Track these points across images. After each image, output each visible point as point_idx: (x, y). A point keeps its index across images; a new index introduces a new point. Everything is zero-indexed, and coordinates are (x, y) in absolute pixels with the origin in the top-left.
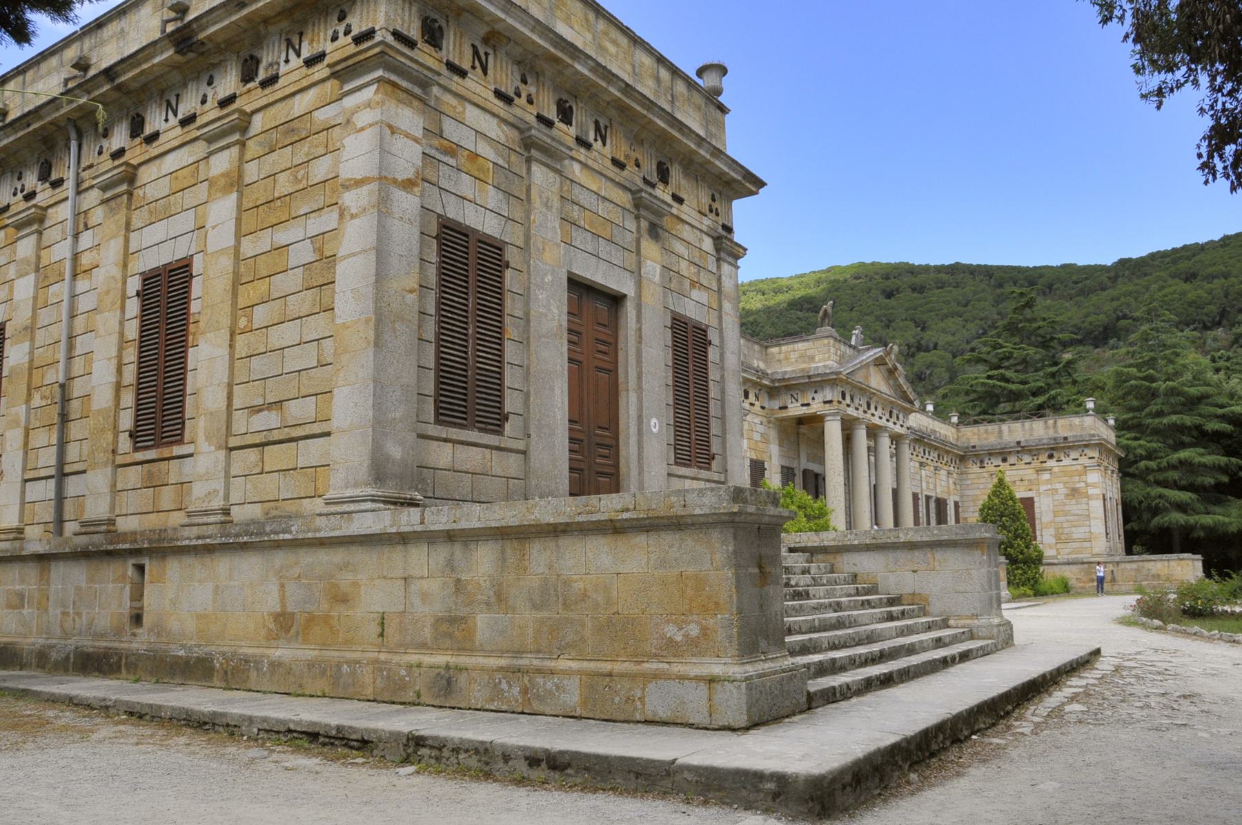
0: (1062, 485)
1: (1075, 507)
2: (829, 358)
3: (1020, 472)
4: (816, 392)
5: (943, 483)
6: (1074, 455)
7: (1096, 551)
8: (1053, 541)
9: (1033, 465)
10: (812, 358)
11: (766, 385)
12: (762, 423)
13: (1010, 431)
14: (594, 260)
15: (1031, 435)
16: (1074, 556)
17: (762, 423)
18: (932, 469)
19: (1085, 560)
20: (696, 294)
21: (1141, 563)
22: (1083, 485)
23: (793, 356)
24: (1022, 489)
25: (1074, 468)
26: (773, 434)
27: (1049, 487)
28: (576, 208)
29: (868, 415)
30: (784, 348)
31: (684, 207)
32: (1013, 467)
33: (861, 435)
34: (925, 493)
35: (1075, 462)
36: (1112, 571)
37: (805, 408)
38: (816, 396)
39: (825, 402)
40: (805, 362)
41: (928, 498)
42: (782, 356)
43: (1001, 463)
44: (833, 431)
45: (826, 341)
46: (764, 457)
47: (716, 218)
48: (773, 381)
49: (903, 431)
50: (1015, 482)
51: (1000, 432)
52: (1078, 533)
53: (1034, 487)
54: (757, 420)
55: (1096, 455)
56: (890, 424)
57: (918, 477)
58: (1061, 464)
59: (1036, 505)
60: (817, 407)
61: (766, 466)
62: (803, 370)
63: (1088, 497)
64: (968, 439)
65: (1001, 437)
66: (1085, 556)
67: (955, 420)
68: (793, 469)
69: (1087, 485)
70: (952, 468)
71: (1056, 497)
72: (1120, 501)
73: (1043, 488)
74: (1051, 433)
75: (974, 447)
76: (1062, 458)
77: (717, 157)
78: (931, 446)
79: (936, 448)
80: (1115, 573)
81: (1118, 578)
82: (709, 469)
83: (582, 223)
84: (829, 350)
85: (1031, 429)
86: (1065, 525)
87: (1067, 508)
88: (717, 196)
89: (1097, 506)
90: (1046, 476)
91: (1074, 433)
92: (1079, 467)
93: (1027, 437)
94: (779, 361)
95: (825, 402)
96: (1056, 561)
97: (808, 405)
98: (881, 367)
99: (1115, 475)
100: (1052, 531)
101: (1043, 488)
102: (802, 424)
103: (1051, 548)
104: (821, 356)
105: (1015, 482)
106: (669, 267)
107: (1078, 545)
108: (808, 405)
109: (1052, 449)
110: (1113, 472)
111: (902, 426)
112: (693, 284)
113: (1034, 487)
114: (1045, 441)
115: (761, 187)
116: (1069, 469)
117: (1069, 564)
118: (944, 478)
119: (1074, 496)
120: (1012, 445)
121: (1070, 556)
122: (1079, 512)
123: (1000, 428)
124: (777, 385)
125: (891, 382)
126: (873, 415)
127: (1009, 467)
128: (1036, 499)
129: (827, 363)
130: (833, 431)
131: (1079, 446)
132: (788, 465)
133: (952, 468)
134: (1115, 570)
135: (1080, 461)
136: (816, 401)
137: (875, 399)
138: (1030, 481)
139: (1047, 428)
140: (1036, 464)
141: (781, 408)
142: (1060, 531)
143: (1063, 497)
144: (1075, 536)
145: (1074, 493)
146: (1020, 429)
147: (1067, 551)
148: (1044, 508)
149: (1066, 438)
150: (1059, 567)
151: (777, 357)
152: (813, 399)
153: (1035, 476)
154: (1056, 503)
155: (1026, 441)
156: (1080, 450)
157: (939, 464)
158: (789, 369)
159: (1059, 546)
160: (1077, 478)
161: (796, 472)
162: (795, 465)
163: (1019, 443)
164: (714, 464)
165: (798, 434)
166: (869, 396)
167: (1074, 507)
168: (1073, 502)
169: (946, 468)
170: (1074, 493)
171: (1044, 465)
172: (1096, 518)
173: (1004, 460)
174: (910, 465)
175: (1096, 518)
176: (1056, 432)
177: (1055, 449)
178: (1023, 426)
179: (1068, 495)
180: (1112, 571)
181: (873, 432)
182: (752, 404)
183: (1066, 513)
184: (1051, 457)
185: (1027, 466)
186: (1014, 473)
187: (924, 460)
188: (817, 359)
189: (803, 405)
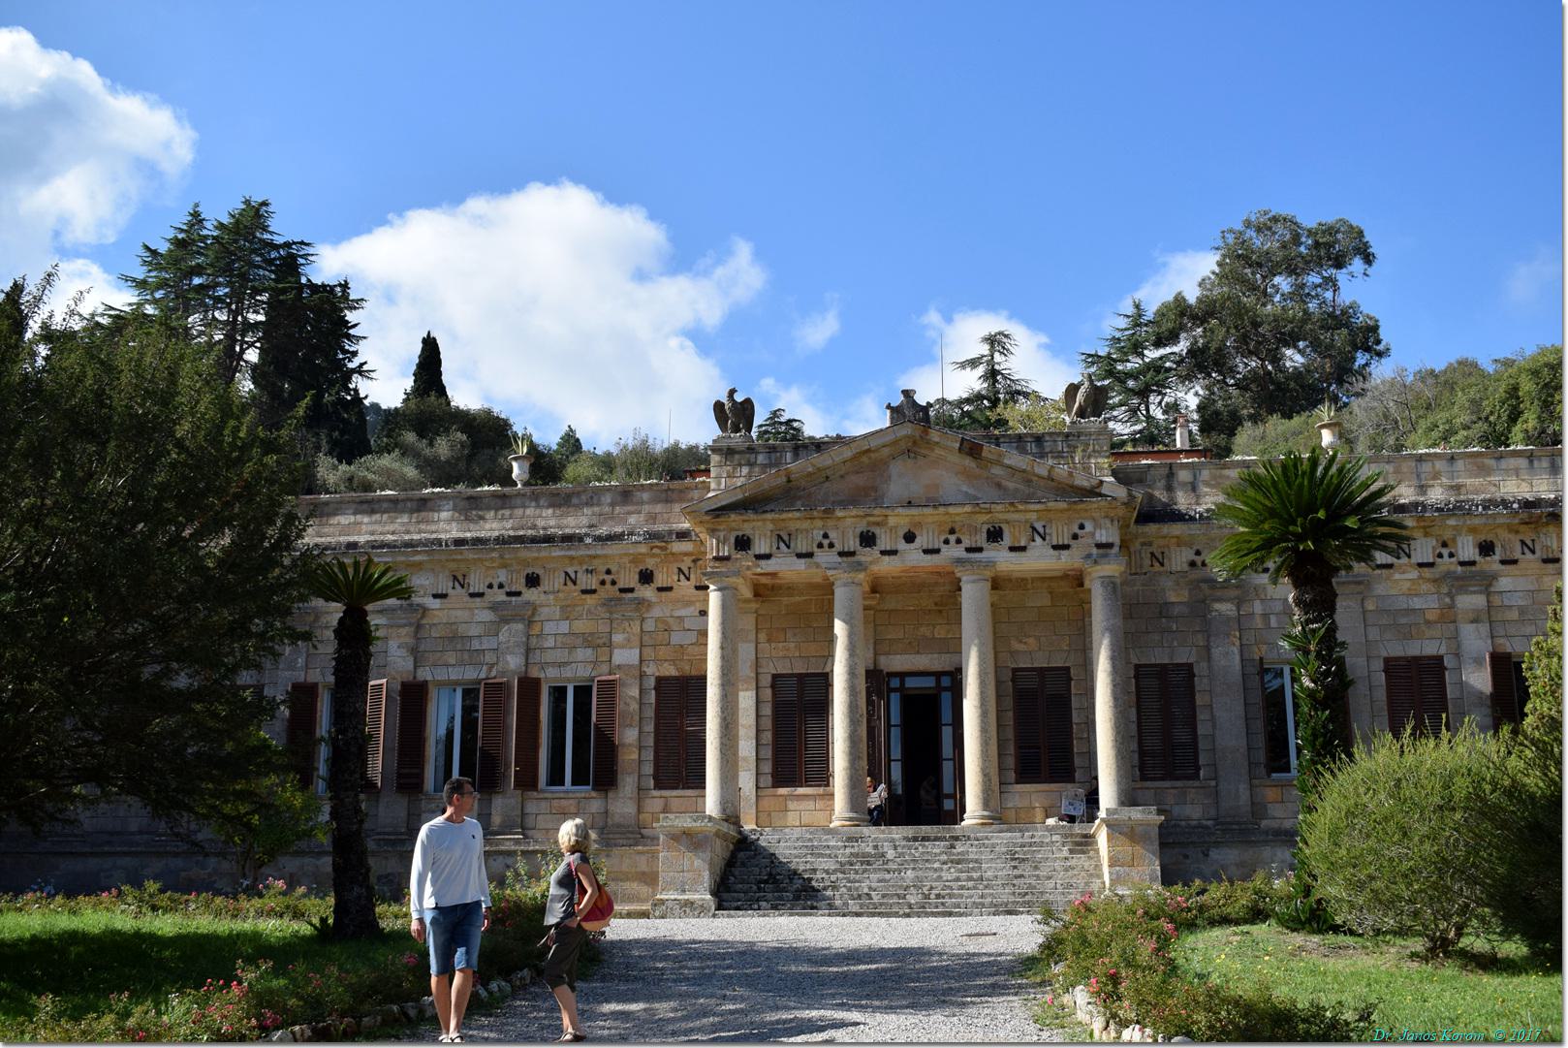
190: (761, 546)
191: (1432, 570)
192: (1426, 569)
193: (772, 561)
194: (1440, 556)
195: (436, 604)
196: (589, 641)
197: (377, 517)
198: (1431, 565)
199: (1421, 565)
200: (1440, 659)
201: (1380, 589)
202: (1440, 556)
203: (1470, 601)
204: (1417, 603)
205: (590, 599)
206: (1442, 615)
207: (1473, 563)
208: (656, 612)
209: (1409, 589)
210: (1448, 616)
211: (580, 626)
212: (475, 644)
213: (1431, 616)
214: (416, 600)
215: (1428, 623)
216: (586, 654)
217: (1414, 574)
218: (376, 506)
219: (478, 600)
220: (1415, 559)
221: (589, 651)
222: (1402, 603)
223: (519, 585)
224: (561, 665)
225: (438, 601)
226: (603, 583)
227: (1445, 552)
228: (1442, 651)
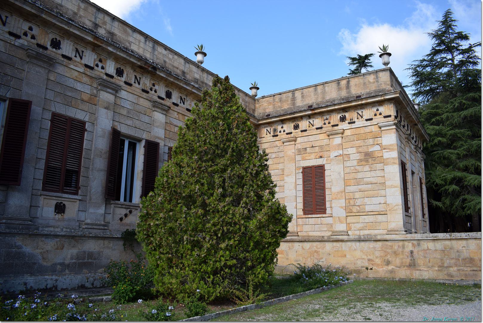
0: (354, 150)
1: (368, 174)
3: (311, 138)
6: (367, 113)
7: (392, 226)
8: (343, 213)
9: (324, 130)
13: (303, 97)
15: (323, 98)
16: (367, 232)
19: (379, 237)
21: (447, 242)
22: (377, 148)
24: (313, 156)
25: (367, 130)
27: (341, 152)
32: (305, 134)
35: (369, 123)
36: (412, 252)
43: (293, 131)
50: (306, 149)
52: (372, 204)
53: (325, 154)
58: (353, 126)
59: (327, 173)
63: (384, 162)
64: (265, 109)
65: (294, 104)
66: (379, 232)
69: (383, 148)
71: (348, 164)
73: (333, 154)
74: (344, 94)
80: (415, 253)
81: (420, 262)
86: (357, 195)
87: (360, 175)
89: (395, 171)
90: (337, 140)
92: (375, 129)
96: (345, 238)
100: (342, 202)
101: (333, 154)
103: (341, 222)
105: (306, 149)
107: (371, 219)
113: (325, 154)
116: (362, 131)
117: (359, 240)
119: (367, 161)
121: (363, 233)
122: (373, 180)
127: (300, 134)
128: (326, 167)
134: (415, 251)
135: (374, 122)
138: (321, 147)
140: (327, 128)
142: (352, 202)
143: (355, 163)
144: (368, 208)
146: (312, 94)
147: (359, 226)
150: (349, 244)
153: (326, 142)
154: (347, 170)
156: (375, 109)
159: (350, 220)
160: (371, 141)
168: (367, 168)
171: (336, 128)
172: (392, 187)
173: (296, 127)
175: (392, 187)
176: (349, 92)
179: (360, 160)
180: (412, 252)
183: (358, 182)
184: (343, 119)
186: (306, 139)
191: (91, 71)
192: (88, 70)
194: (97, 66)
198: (92, 68)
199: (86, 66)
200: (83, 123)
201: (60, 69)
202: (97, 66)
203: (106, 96)
204: (79, 87)
206: (90, 99)
207: (112, 77)
209: (76, 77)
210: (93, 100)
213: (85, 97)
215: (82, 100)
217: (82, 69)
220: (83, 62)
222: (71, 83)
227: (100, 65)
228: (86, 119)
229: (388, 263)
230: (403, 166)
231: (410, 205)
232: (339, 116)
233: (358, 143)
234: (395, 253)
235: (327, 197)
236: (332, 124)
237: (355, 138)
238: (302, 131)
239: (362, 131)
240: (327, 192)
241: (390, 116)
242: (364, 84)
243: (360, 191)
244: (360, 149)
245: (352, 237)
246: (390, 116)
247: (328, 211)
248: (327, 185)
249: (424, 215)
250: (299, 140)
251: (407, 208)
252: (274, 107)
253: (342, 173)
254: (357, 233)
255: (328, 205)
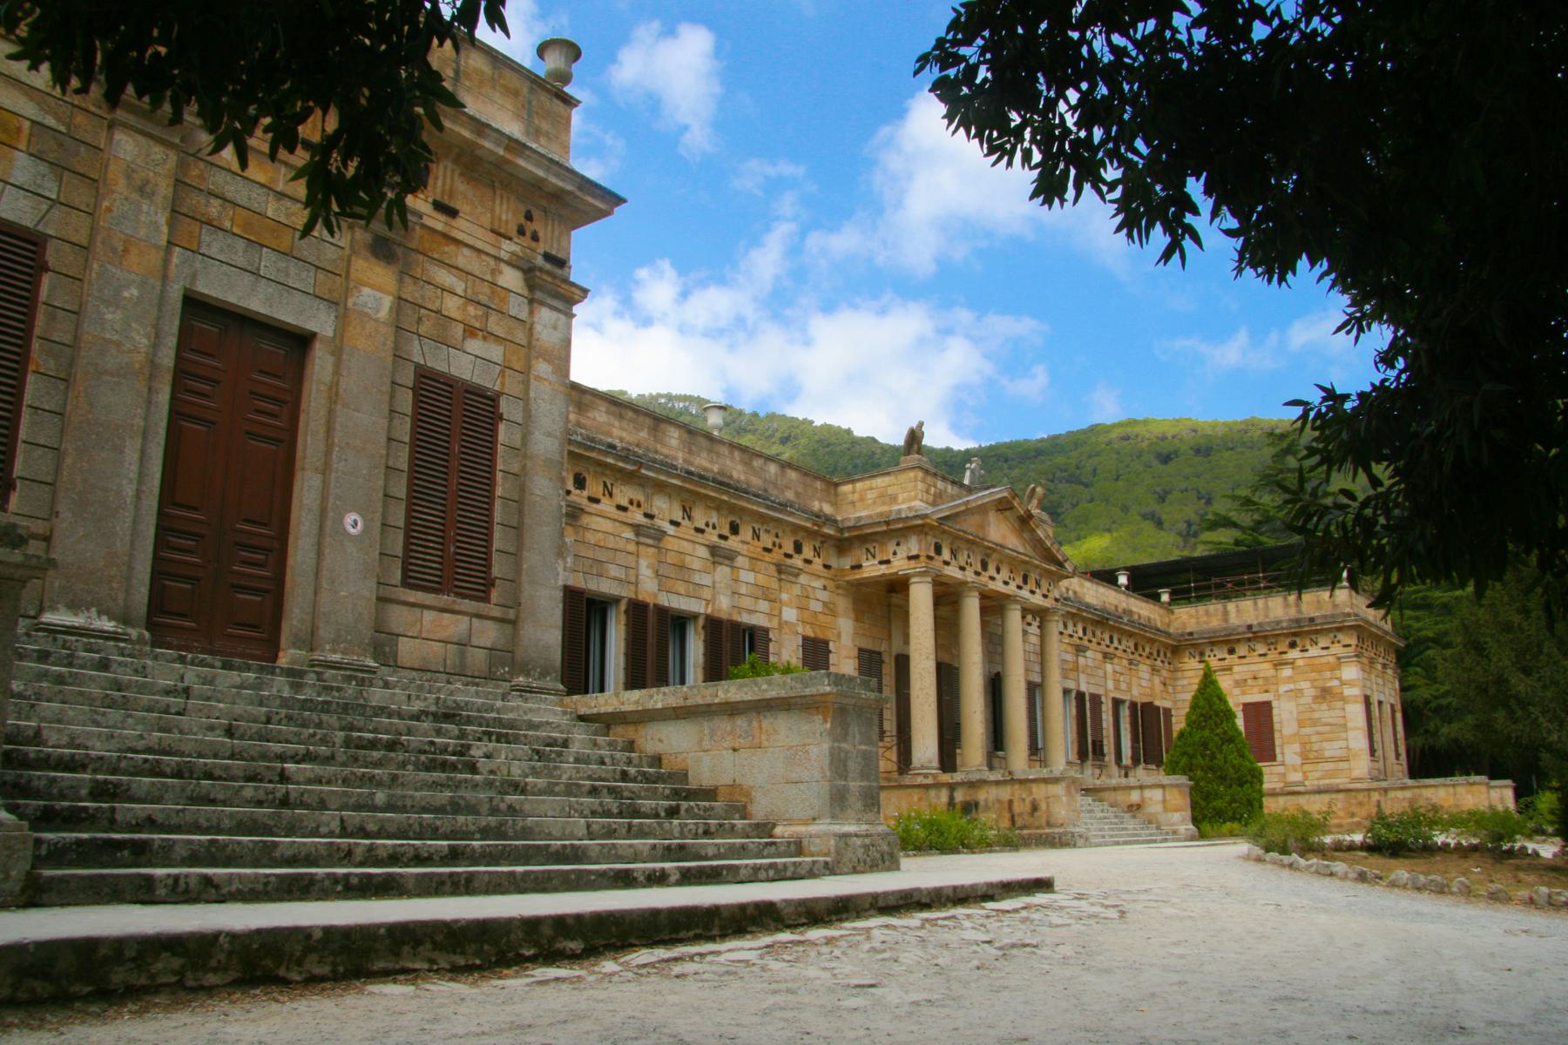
1: (1327, 714)
2: (915, 498)
3: (1253, 667)
4: (898, 544)
5: (1144, 683)
6: (1323, 642)
7: (1356, 773)
8: (1298, 761)
9: (1269, 657)
10: (894, 499)
11: (830, 536)
12: (825, 588)
13: (1238, 611)
14: (248, 278)
15: (1267, 616)
16: (1327, 781)
17: (825, 588)
18: (1125, 662)
19: (1341, 787)
20: (474, 346)
21: (1417, 791)
23: (871, 495)
24: (1256, 690)
25: (1324, 660)
26: (843, 603)
27: (1292, 686)
28: (216, 202)
29: (984, 578)
30: (859, 485)
31: (459, 222)
32: (1244, 661)
33: (972, 608)
34: (1112, 695)
35: (1325, 652)
36: (1379, 801)
37: (883, 567)
38: (899, 550)
39: (910, 558)
40: (884, 504)
41: (1117, 703)
42: (856, 497)
43: (1227, 656)
44: (921, 598)
45: (912, 474)
46: (829, 635)
47: (534, 244)
48: (841, 530)
49: (1047, 603)
50: (1246, 680)
51: (1226, 613)
52: (1332, 749)
53: (1272, 688)
54: (818, 584)
55: (1353, 641)
56: (1025, 593)
57: (1101, 673)
58: (1306, 654)
59: (1275, 712)
60: (899, 565)
61: (832, 646)
62: (881, 514)
63: (1344, 699)
64: (1184, 624)
65: (1226, 620)
66: (1341, 781)
67: (1165, 598)
68: (880, 653)
69: (1343, 683)
70: (1159, 663)
71: (1302, 701)
72: (1398, 707)
73: (1283, 688)
74: (1293, 612)
75: (1191, 634)
76: (1308, 647)
77: (520, 155)
78: (1122, 632)
79: (1131, 635)
80: (1382, 804)
82: (486, 600)
83: (227, 224)
84: (916, 486)
85: (1267, 608)
86: (1314, 739)
87: (1316, 715)
88: (536, 213)
89: (1356, 712)
90: (1287, 672)
91: (1323, 612)
92: (1331, 659)
93: (1261, 619)
94: (853, 503)
95: (910, 558)
96: (1301, 789)
97: (888, 562)
98: (1007, 513)
99: (1390, 672)
100: (1297, 747)
101: (1283, 688)
102: (895, 592)
103: (1295, 771)
104: (905, 495)
105: (1246, 680)
106: (420, 302)
107: (1330, 766)
108: (888, 562)
109: (1294, 634)
110: (1384, 666)
111: (1045, 596)
112: (470, 331)
113: (1272, 688)
114: (1284, 625)
115: (617, 205)
116: (1317, 661)
118: (1147, 676)
119: (1324, 698)
120: (1240, 630)
121: (1322, 782)
123: (1225, 608)
124: (846, 535)
125: (1026, 535)
126: (992, 578)
127: (1237, 661)
128: (1274, 704)
129: (913, 504)
130: (921, 598)
131: (1330, 630)
132: (870, 647)
133: (1159, 663)
134: (1382, 799)
136: (899, 556)
137: (995, 556)
138: (1266, 679)
139: (1287, 605)
140: (1273, 655)
141: (853, 568)
142: (1308, 747)
143: (1310, 700)
144: (1327, 754)
145: (1325, 694)
146: (1251, 609)
147: (1317, 774)
148: (1285, 716)
149: (1312, 620)
150: (1307, 797)
151: (850, 497)
152: (895, 553)
153: (1272, 672)
154: (1301, 708)
155: (1260, 624)
156: (1332, 635)
157: (1136, 656)
158: (864, 513)
159: (1306, 768)
160: (1328, 674)
161: (886, 657)
162: (883, 648)
163: (1250, 627)
164: (495, 595)
165: (889, 605)
166: (988, 555)
167: (1325, 713)
168: (1324, 706)
169: (1148, 662)
170: (1325, 694)
171: (1284, 656)
172: (1355, 728)
173: (1231, 651)
174: (1058, 650)
175: (1355, 728)
176: (1299, 611)
177: (1299, 633)
178: (1256, 604)
180: (1379, 801)
181: (993, 606)
182: (808, 561)
184: (1293, 645)
185: (1262, 659)
186: (1245, 668)
187: (1111, 650)
188: (900, 498)
189: (881, 563)
190: (946, 555)
193: (950, 568)
195: (671, 530)
196: (766, 594)
197: (624, 424)
205: (767, 557)
208: (803, 579)
211: (761, 579)
212: (697, 578)
214: (657, 522)
216: (764, 605)
218: (623, 412)
219: (700, 535)
221: (766, 603)
223: (726, 532)
224: (751, 612)
225: (673, 527)
226: (774, 544)
229: (1353, 815)
230: (1367, 701)
231: (1377, 746)
232: (1288, 640)
233: (1314, 675)
234: (1361, 804)
235: (1278, 742)
236: (1280, 650)
237: (1308, 668)
238: (1240, 657)
239: (1317, 661)
240: (1277, 735)
241: (1349, 646)
242: (1318, 602)
243: (1318, 733)
244: (1316, 684)
245: (1309, 788)
246: (1349, 646)
247: (1279, 757)
248: (1276, 726)
249: (1398, 756)
250: (1236, 669)
251: (1372, 751)
252: (1198, 623)
253: (1295, 712)
254: (1316, 782)
255: (1278, 750)
